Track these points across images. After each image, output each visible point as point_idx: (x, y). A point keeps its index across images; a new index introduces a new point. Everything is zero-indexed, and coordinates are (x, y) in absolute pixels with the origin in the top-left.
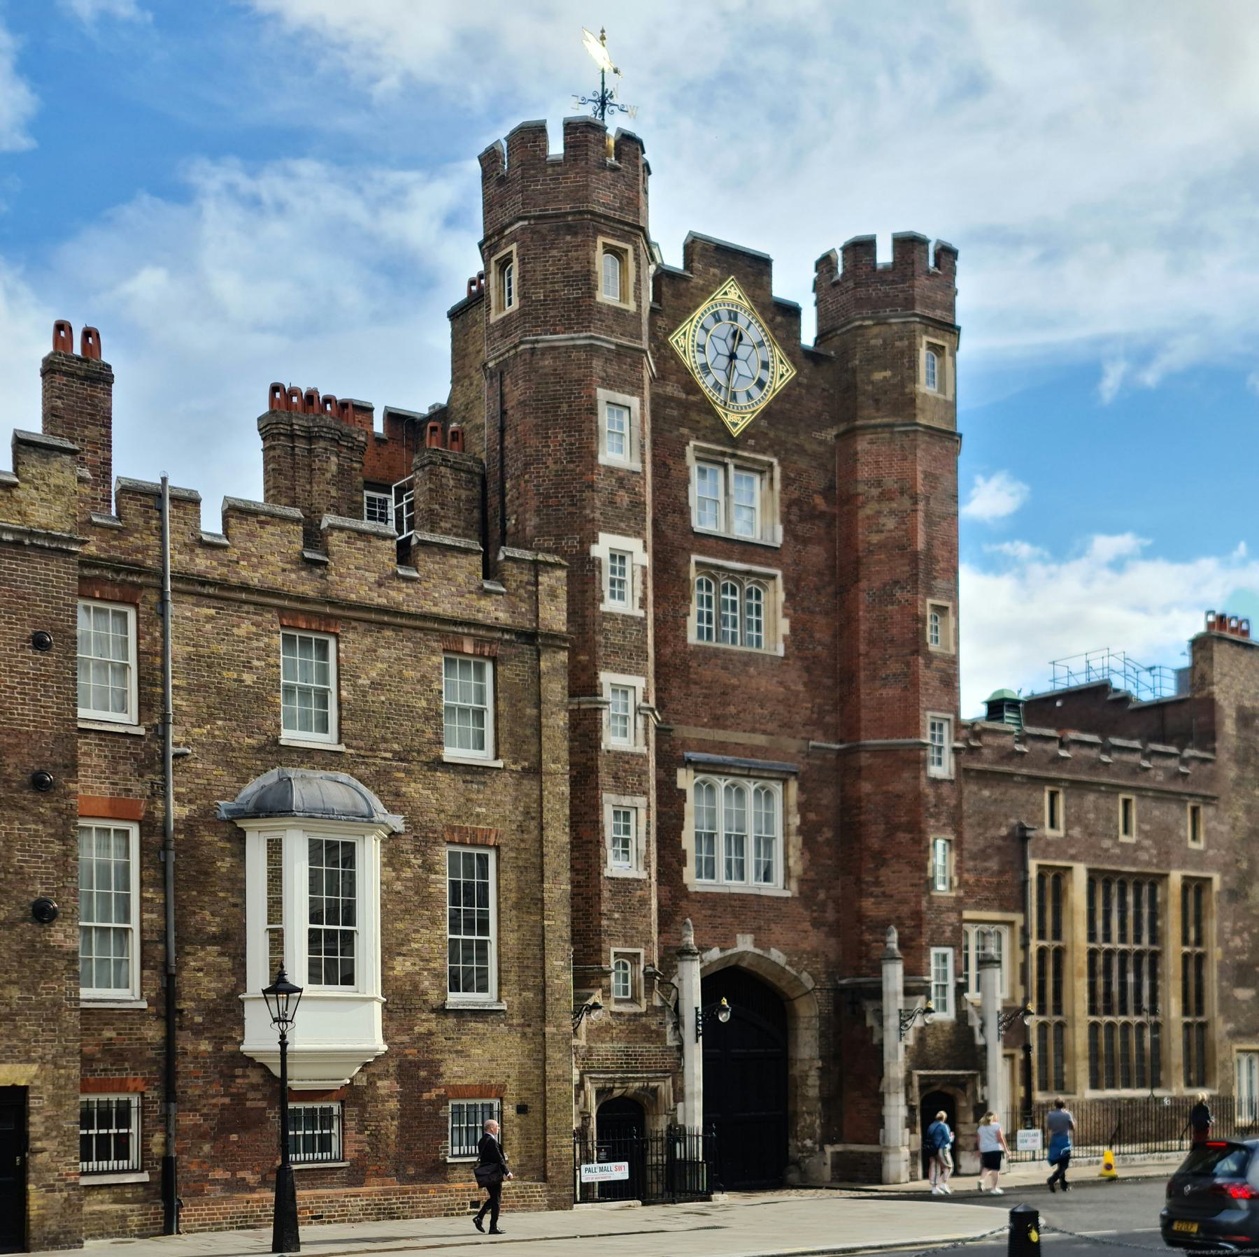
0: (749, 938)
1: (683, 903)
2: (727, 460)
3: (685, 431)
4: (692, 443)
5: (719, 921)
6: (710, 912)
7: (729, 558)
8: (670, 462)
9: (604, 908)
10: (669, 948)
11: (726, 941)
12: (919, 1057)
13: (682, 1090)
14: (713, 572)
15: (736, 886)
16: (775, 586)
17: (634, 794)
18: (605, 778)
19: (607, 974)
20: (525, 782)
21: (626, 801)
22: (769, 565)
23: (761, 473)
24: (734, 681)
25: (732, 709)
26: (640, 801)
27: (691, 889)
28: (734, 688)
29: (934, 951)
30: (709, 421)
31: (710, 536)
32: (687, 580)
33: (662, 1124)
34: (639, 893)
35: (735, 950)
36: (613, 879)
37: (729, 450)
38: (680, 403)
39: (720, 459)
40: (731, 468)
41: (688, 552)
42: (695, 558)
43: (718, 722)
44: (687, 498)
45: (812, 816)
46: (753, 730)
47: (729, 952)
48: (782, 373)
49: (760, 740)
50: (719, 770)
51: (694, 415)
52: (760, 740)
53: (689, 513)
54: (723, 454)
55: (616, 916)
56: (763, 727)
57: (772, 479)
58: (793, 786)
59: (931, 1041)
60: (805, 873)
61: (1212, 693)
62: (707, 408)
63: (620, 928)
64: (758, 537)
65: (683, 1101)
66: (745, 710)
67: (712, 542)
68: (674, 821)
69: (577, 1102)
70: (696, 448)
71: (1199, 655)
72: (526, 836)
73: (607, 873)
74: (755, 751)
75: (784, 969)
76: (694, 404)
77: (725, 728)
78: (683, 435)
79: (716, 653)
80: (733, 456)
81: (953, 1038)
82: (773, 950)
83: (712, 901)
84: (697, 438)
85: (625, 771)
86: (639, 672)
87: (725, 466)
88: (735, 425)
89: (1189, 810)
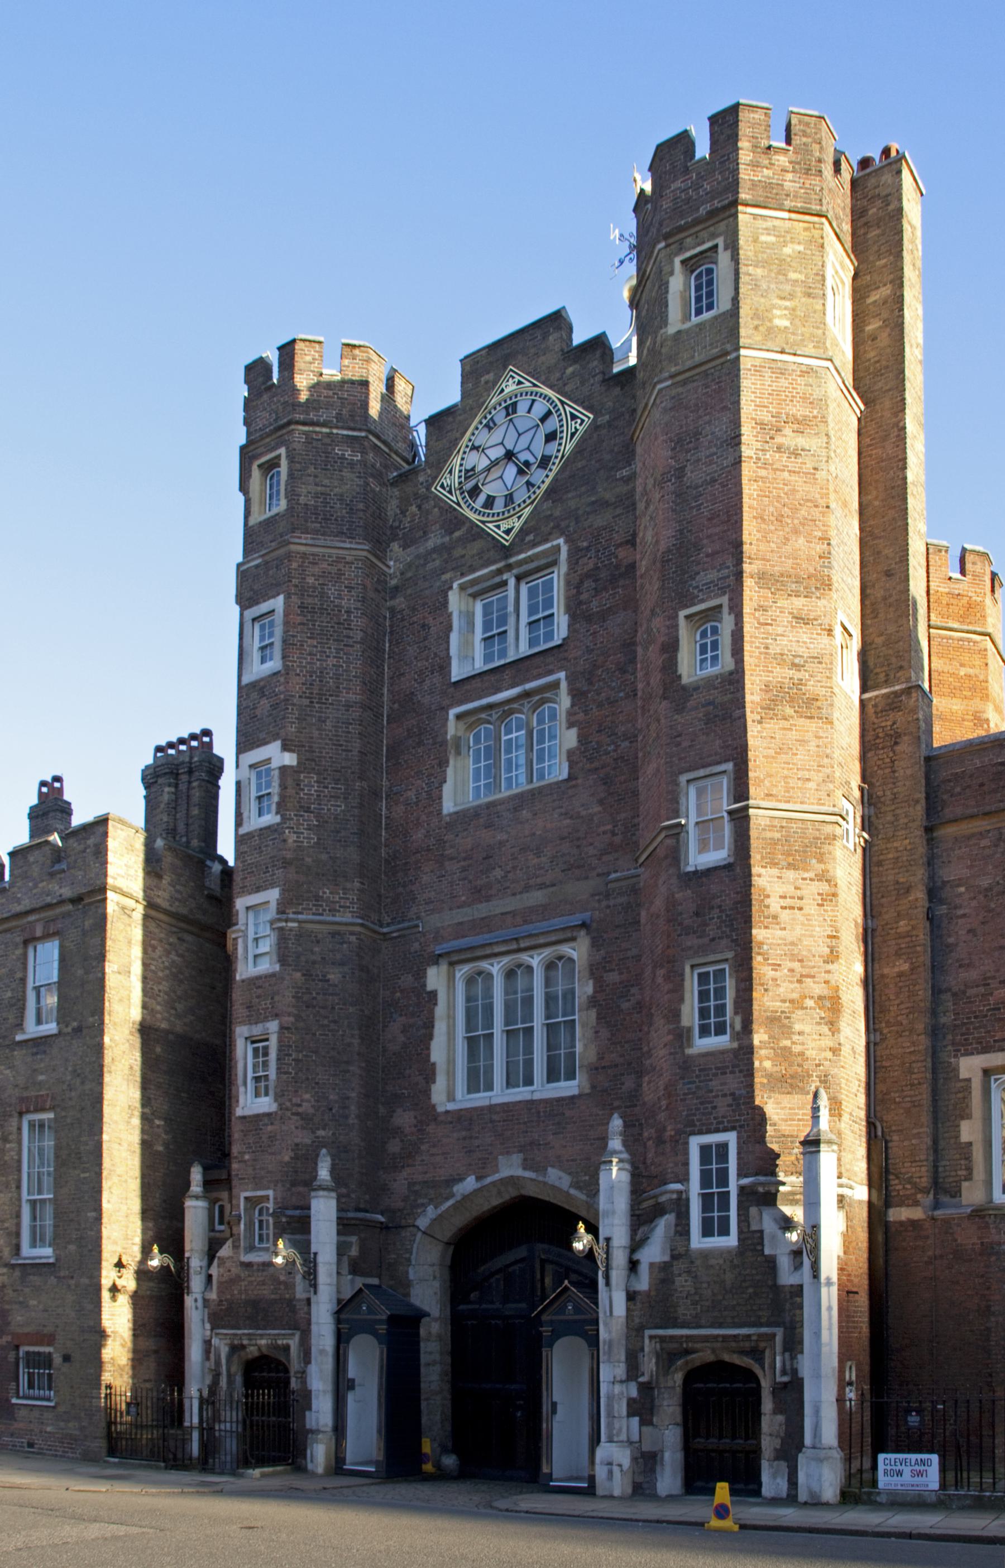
0: (517, 1158)
1: (431, 1128)
5: (477, 1142)
6: (464, 1133)
7: (498, 690)
8: (430, 621)
9: (235, 1150)
10: (415, 1183)
11: (483, 1166)
12: (653, 1308)
14: (483, 716)
15: (521, 1093)
17: (266, 1019)
18: (238, 1010)
20: (74, 1042)
21: (257, 1030)
24: (501, 836)
25: (498, 873)
26: (273, 1026)
27: (440, 1109)
28: (501, 843)
29: (695, 1142)
31: (473, 677)
32: (444, 743)
34: (270, 1128)
35: (497, 1177)
36: (244, 1117)
41: (445, 709)
42: (453, 712)
43: (480, 894)
44: (448, 649)
45: (613, 977)
46: (527, 888)
47: (489, 1180)
49: (536, 897)
50: (479, 953)
52: (536, 897)
53: (450, 664)
55: (247, 1157)
56: (539, 880)
59: (682, 1283)
60: (601, 1057)
63: (250, 1171)
66: (514, 868)
67: (477, 684)
68: (423, 1031)
72: (73, 1094)
73: (239, 1112)
74: (528, 915)
75: (567, 1192)
77: (488, 899)
81: (729, 1277)
82: (550, 1169)
83: (464, 1119)
85: (258, 997)
86: (272, 886)
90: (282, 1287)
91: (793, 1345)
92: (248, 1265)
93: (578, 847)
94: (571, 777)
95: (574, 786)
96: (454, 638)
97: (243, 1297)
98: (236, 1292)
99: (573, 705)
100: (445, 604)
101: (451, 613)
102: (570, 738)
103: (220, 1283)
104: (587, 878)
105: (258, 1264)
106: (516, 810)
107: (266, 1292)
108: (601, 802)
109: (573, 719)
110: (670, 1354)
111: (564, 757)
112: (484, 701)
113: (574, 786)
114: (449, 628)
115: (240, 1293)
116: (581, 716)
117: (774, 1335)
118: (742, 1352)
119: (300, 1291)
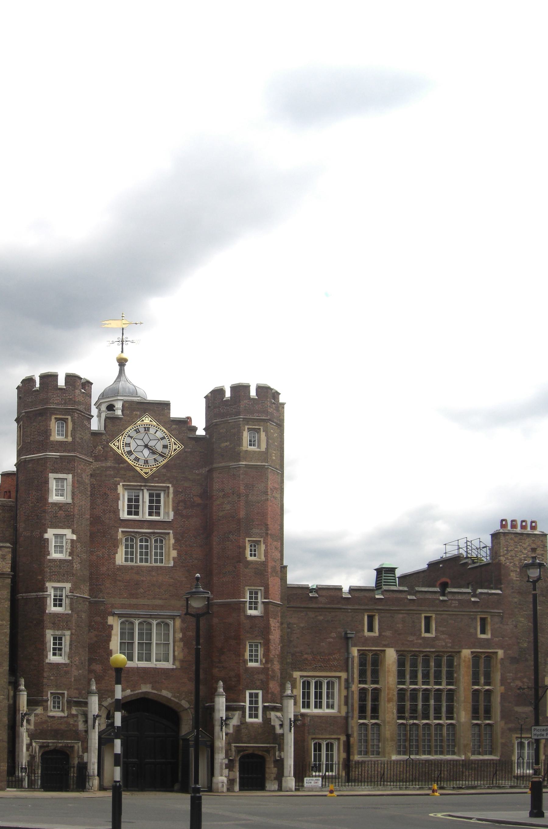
2: (142, 488)
3: (118, 479)
4: (121, 484)
13: (87, 748)
16: (169, 537)
19: (47, 701)
22: (166, 529)
23: (164, 491)
30: (132, 474)
33: (76, 762)
37: (142, 484)
38: (114, 468)
39: (138, 488)
40: (145, 491)
41: (118, 528)
44: (118, 506)
48: (175, 447)
49: (159, 602)
51: (122, 472)
54: (141, 486)
57: (168, 493)
58: (178, 622)
61: (500, 560)
62: (130, 468)
64: (162, 518)
65: (87, 752)
69: (28, 749)
70: (123, 485)
71: (495, 541)
76: (122, 467)
78: (116, 481)
79: (132, 568)
80: (145, 486)
84: (124, 481)
87: (143, 490)
88: (146, 473)
89: (479, 620)
90: (71, 726)
91: (281, 749)
92: (53, 717)
93: (176, 590)
94: (174, 566)
95: (176, 570)
96: (120, 503)
97: (49, 728)
98: (45, 726)
99: (175, 543)
100: (116, 489)
101: (119, 494)
102: (174, 554)
103: (36, 724)
104: (179, 600)
105: (58, 717)
106: (150, 571)
107: (63, 727)
108: (186, 577)
109: (175, 547)
110: (239, 750)
111: (171, 559)
112: (136, 530)
113: (176, 570)
114: (119, 499)
115: (48, 726)
116: (179, 547)
117: (276, 747)
118: (263, 751)
119: (81, 726)
